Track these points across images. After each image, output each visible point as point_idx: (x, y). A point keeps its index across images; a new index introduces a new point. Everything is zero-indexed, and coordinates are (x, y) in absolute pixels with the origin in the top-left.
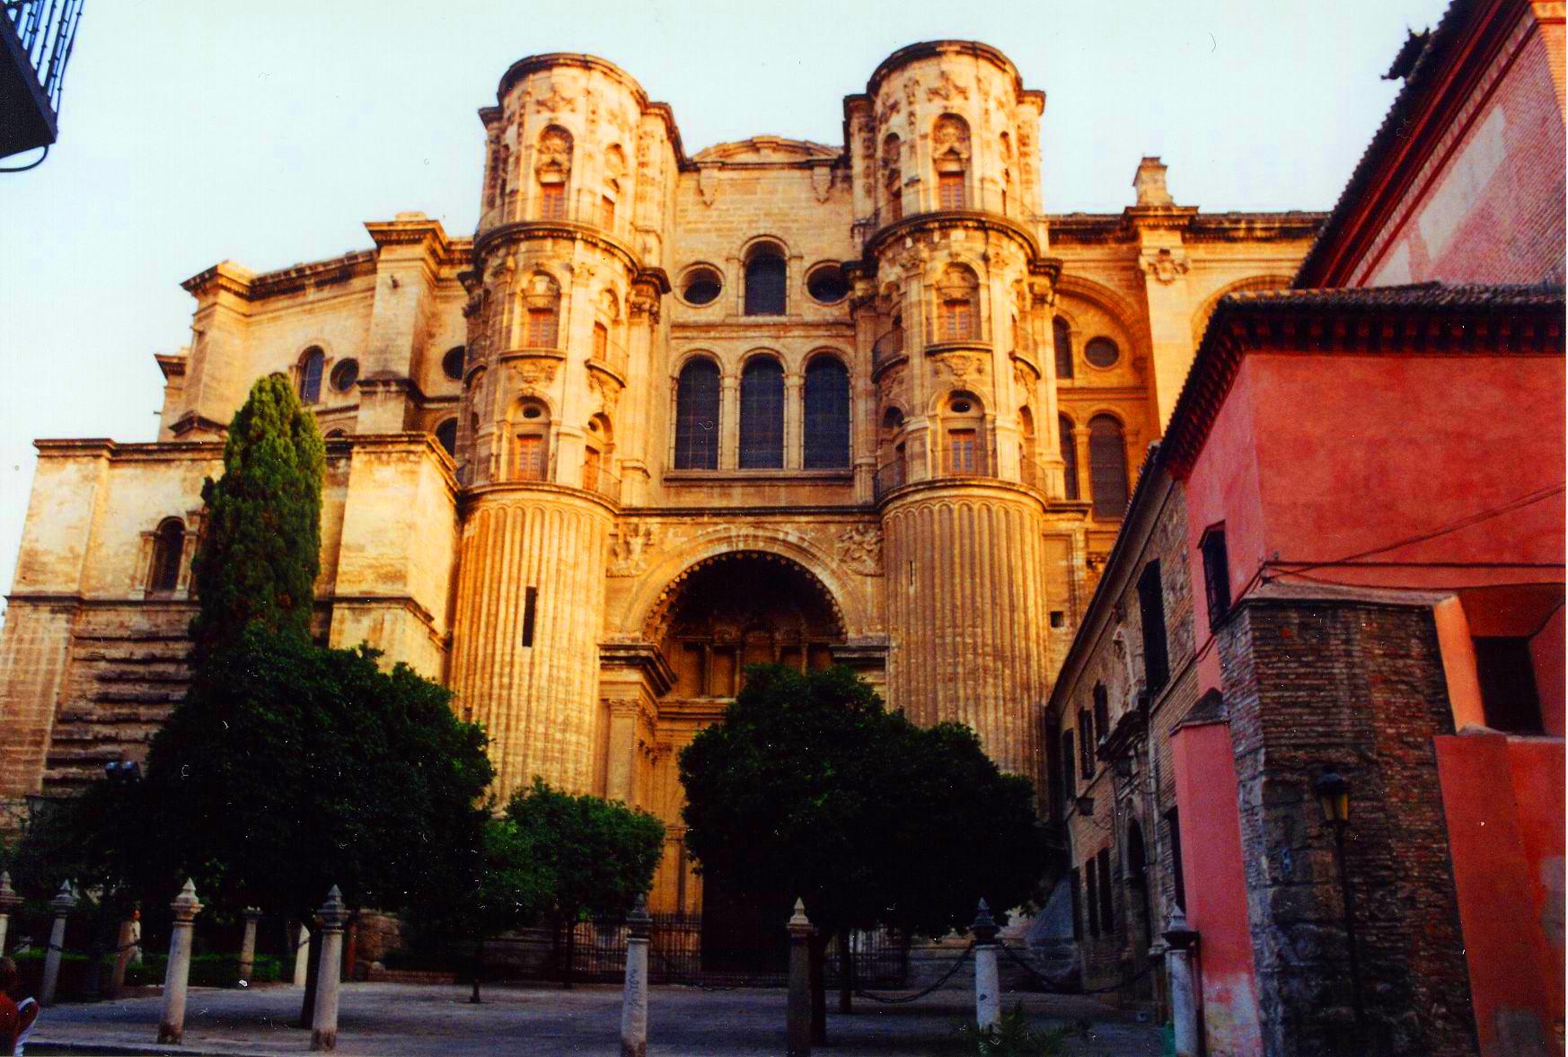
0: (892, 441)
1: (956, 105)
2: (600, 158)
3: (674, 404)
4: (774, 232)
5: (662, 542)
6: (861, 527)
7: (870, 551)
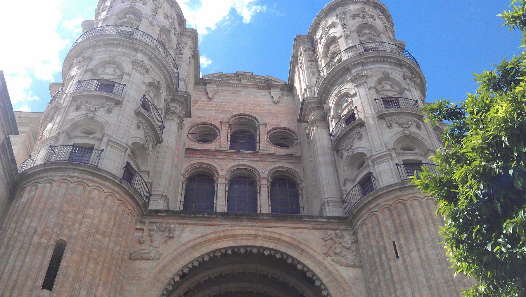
0: (353, 181)
1: (370, 20)
2: (157, 30)
3: (184, 191)
4: (249, 113)
5: (179, 236)
6: (338, 231)
7: (348, 249)
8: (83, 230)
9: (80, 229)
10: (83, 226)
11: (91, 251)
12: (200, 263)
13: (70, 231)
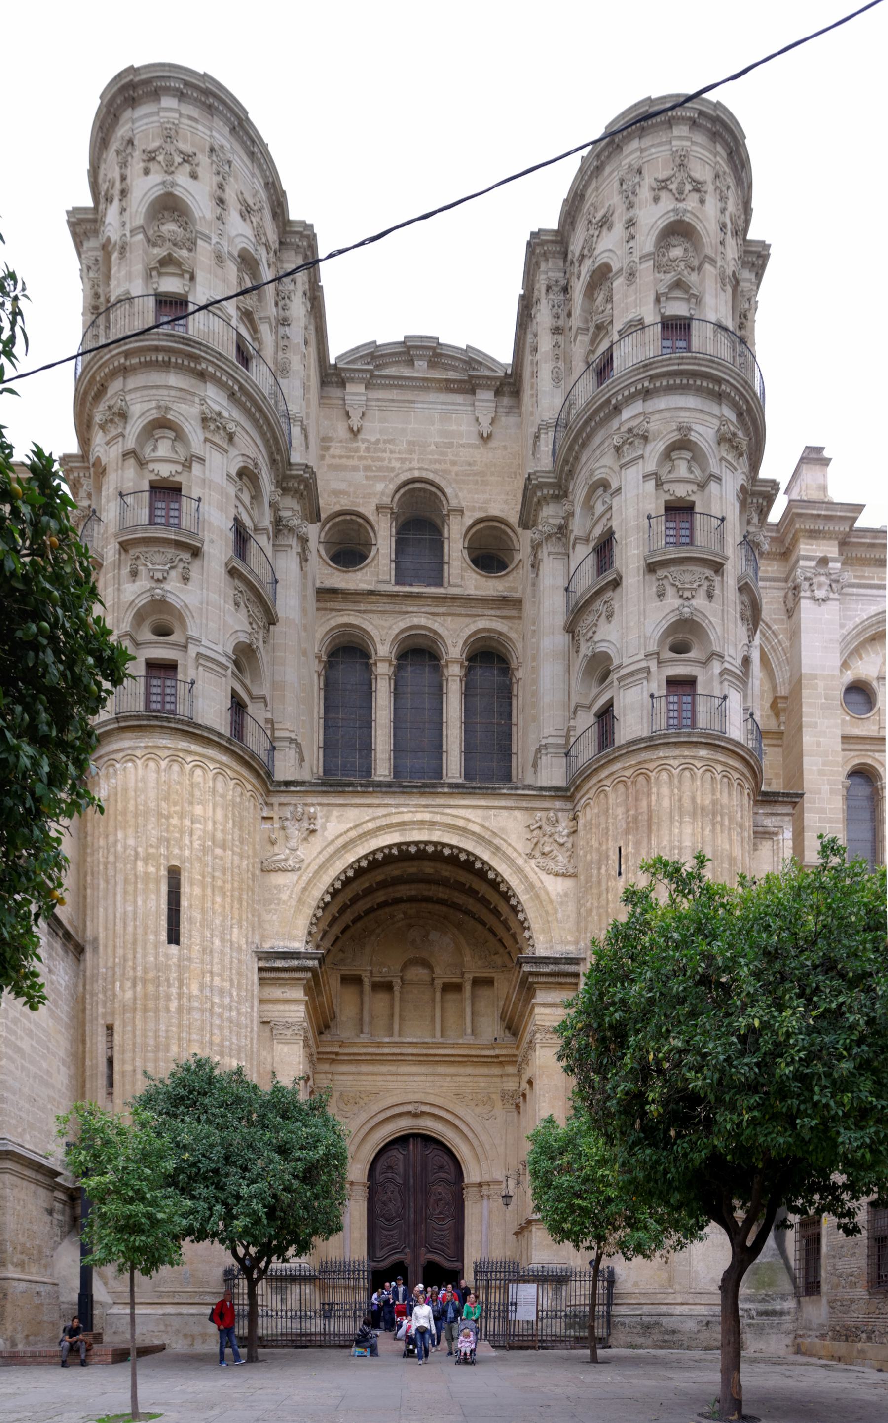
8: (196, 845)
9: (191, 842)
10: (195, 837)
11: (213, 877)
12: (356, 871)
13: (181, 848)
